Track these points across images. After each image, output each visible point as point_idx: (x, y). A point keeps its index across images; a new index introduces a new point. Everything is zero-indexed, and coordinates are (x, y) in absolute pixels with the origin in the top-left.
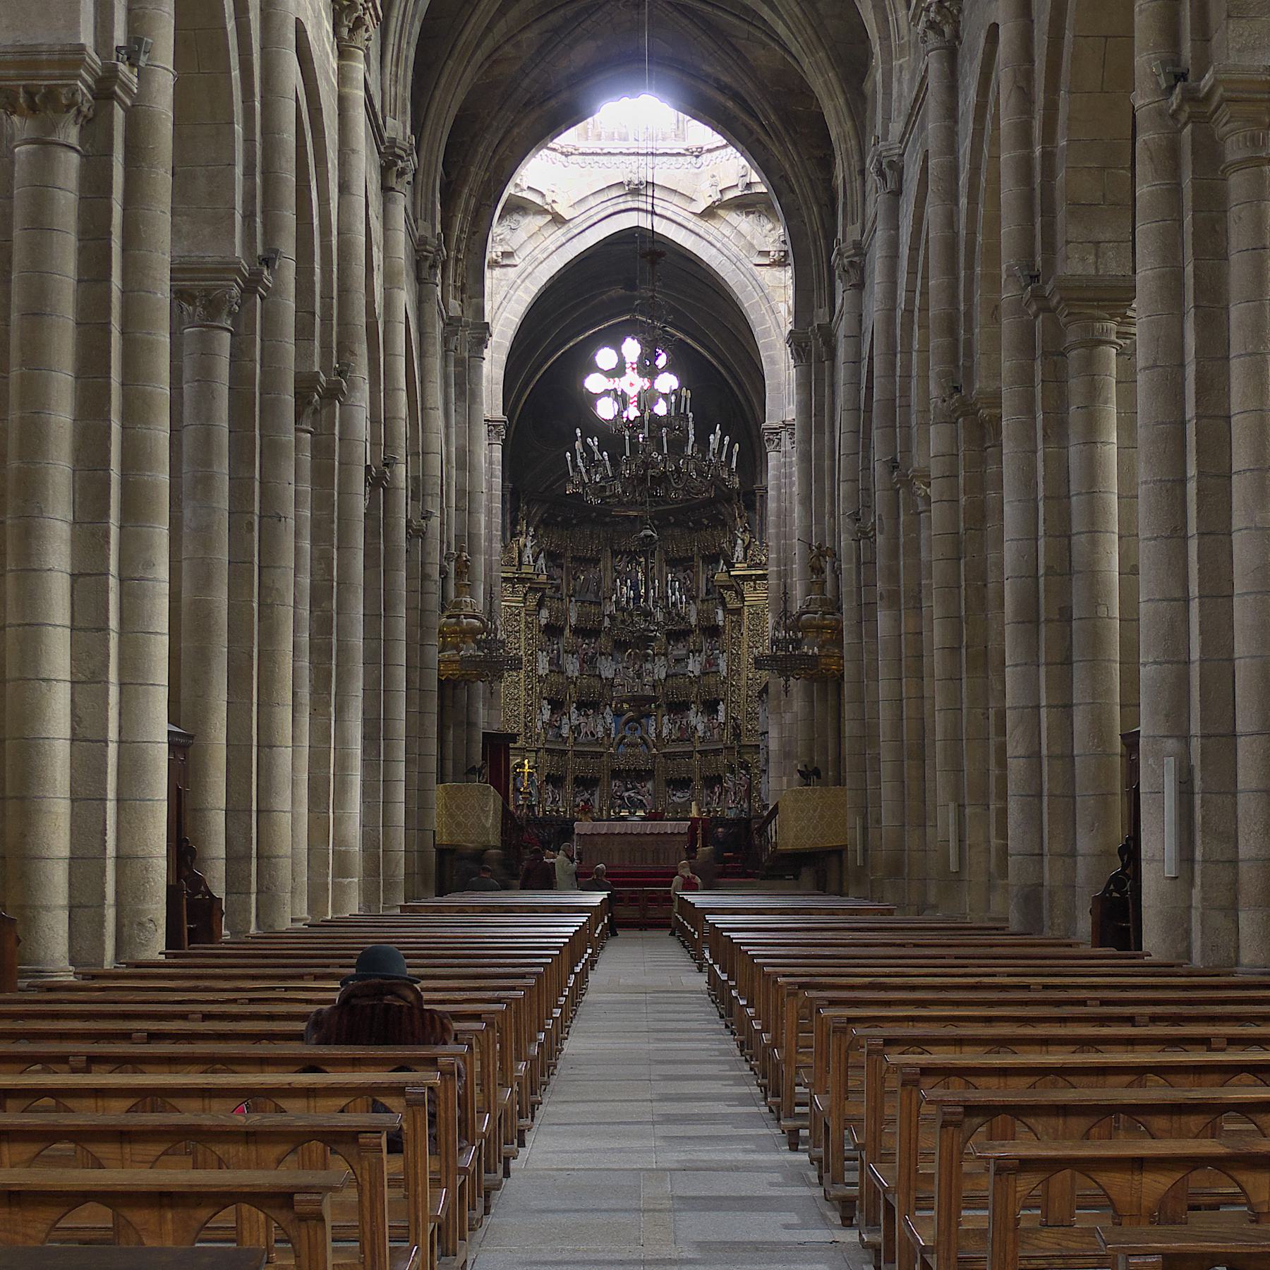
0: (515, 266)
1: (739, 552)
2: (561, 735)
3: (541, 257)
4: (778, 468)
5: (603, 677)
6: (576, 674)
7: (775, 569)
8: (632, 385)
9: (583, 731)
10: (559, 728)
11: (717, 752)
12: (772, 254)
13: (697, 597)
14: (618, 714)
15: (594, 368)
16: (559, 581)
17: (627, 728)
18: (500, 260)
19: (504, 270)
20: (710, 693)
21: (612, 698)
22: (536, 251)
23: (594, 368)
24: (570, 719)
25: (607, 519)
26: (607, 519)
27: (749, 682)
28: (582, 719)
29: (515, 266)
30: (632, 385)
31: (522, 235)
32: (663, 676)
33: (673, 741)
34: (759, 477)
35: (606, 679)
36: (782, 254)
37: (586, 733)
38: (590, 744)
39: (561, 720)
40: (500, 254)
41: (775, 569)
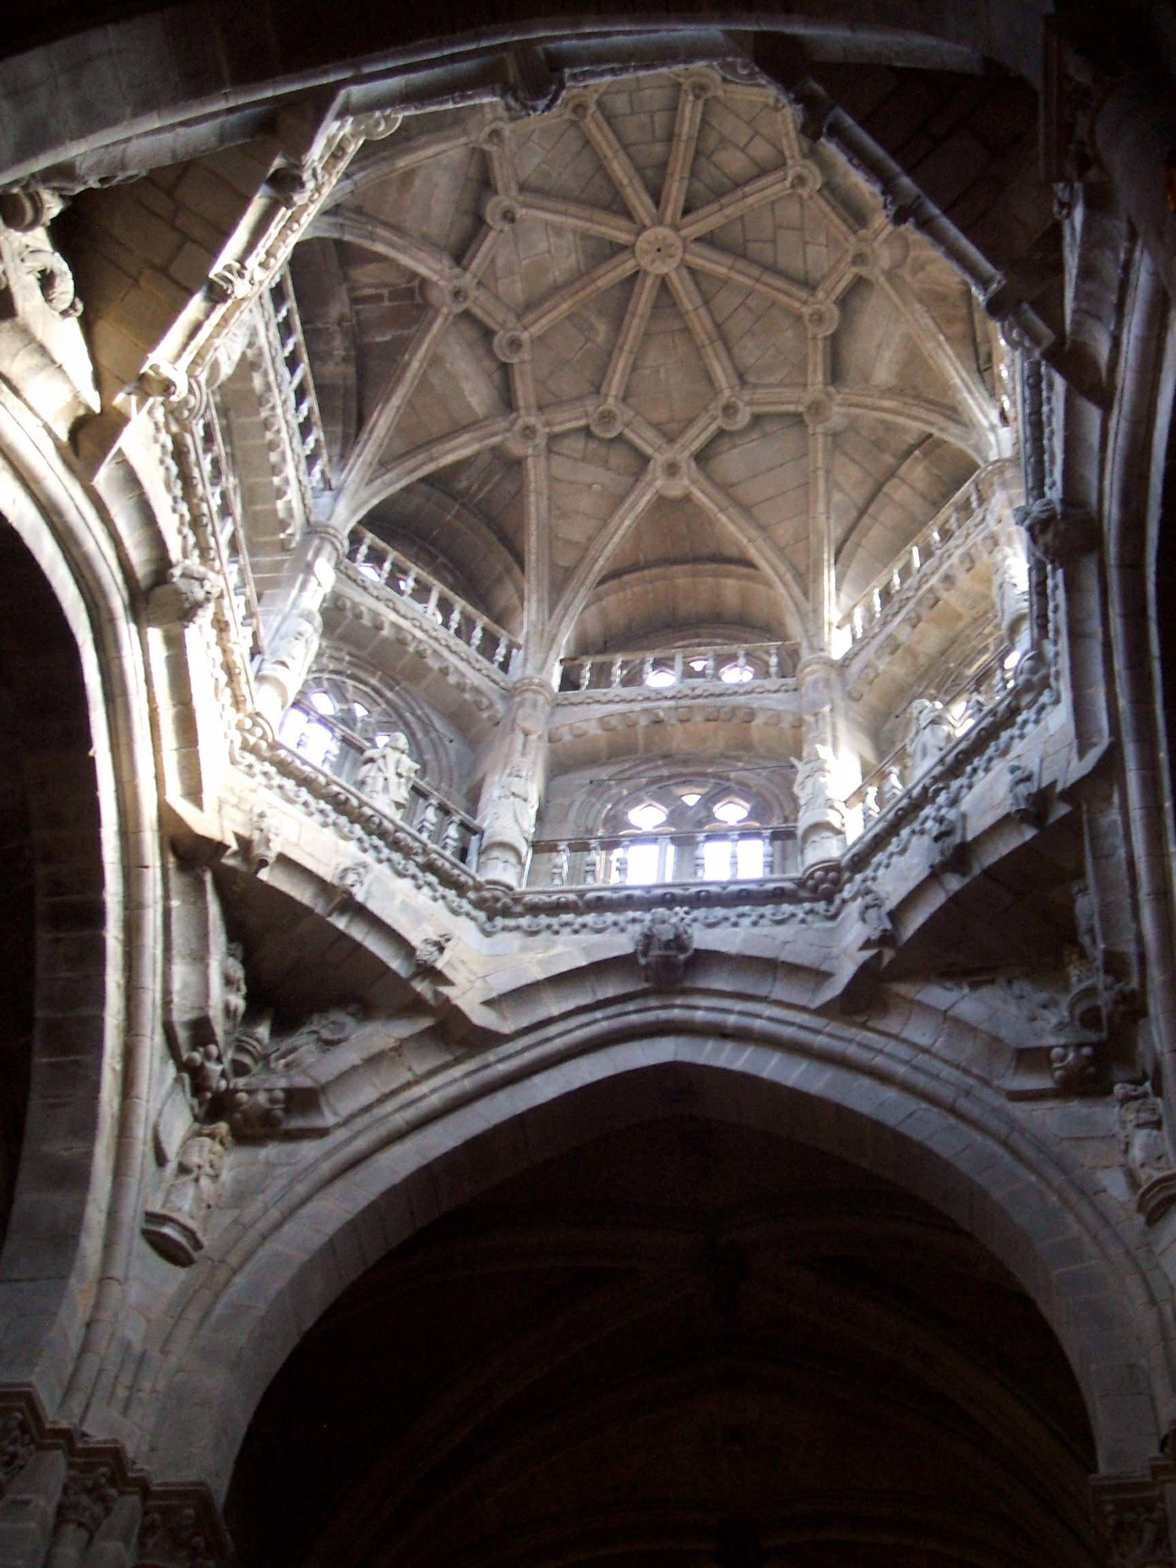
0: (322, 1133)
3: (400, 1120)
12: (1056, 1052)
18: (278, 1111)
19: (290, 1147)
22: (390, 1106)
29: (322, 1133)
31: (347, 1056)
36: (1086, 1051)
40: (280, 1095)
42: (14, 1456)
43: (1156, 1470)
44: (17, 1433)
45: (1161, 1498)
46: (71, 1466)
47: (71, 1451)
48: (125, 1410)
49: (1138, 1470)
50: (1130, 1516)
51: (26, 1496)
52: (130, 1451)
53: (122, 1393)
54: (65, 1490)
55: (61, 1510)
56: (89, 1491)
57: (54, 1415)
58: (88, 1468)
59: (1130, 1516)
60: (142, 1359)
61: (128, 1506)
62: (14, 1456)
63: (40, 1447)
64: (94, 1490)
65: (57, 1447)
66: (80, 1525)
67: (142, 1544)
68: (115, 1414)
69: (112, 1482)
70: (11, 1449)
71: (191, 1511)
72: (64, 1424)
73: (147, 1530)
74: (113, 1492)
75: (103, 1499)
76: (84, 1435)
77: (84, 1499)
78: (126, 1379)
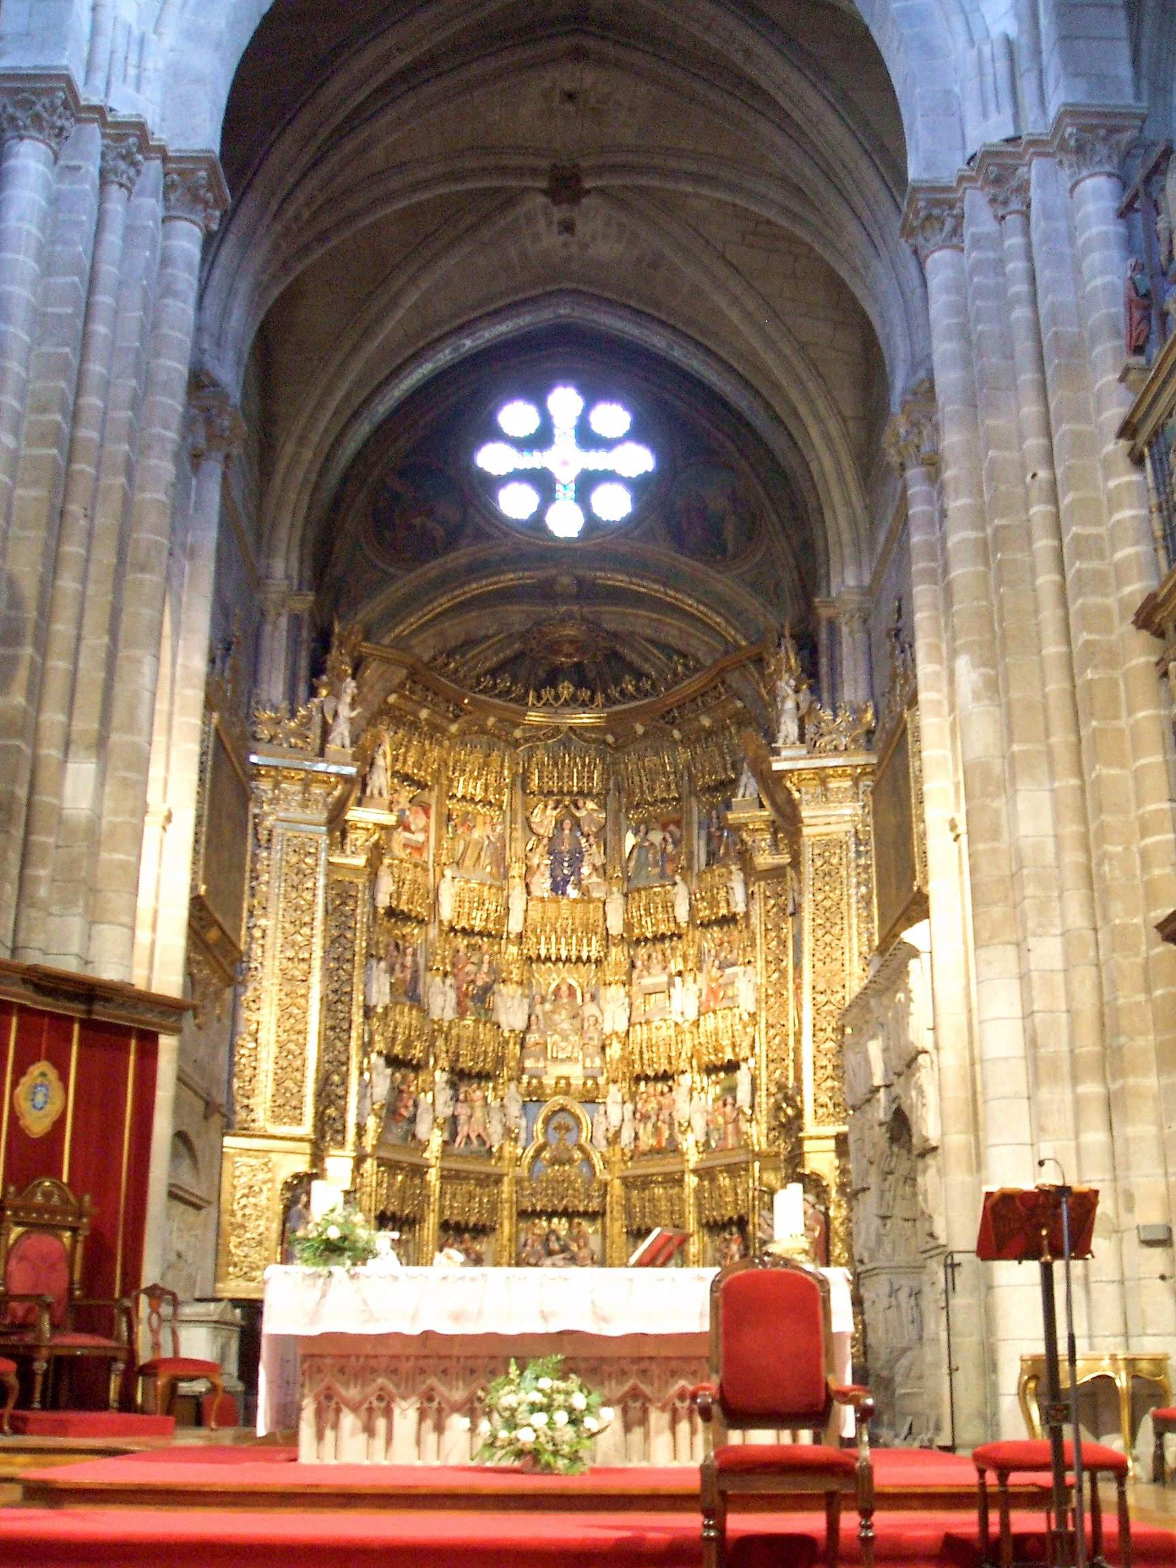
1: (789, 727)
2: (414, 1136)
4: (958, 287)
5: (505, 1026)
6: (449, 1014)
7: (971, 534)
8: (565, 463)
9: (463, 1130)
10: (413, 1120)
11: (733, 1170)
13: (690, 867)
14: (534, 1097)
15: (495, 434)
16: (420, 837)
17: (550, 1130)
20: (717, 1050)
21: (523, 1070)
23: (493, 433)
24: (433, 1104)
25: (518, 733)
26: (518, 733)
27: (821, 999)
28: (463, 1111)
30: (565, 463)
32: (622, 1027)
33: (644, 1154)
34: (824, 584)
35: (512, 1031)
37: (468, 1136)
38: (476, 1156)
39: (416, 1105)
41: (971, 534)
42: (62, 129)
43: (961, 179)
44: (61, 109)
45: (962, 200)
46: (104, 136)
47: (104, 124)
48: (138, 88)
49: (947, 177)
50: (936, 212)
51: (73, 163)
52: (150, 126)
53: (132, 72)
54: (103, 156)
55: (103, 173)
56: (124, 158)
57: (90, 96)
58: (120, 138)
59: (936, 212)
60: (142, 42)
61: (153, 169)
62: (62, 129)
63: (78, 120)
64: (127, 157)
65: (92, 120)
66: (121, 185)
67: (166, 199)
68: (131, 91)
69: (140, 151)
70: (59, 123)
71: (203, 174)
72: (96, 101)
73: (169, 188)
74: (139, 157)
75: (134, 164)
76: (111, 110)
77: (122, 165)
78: (133, 60)
